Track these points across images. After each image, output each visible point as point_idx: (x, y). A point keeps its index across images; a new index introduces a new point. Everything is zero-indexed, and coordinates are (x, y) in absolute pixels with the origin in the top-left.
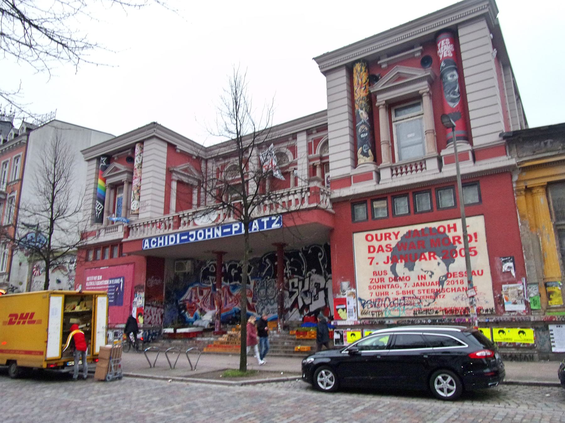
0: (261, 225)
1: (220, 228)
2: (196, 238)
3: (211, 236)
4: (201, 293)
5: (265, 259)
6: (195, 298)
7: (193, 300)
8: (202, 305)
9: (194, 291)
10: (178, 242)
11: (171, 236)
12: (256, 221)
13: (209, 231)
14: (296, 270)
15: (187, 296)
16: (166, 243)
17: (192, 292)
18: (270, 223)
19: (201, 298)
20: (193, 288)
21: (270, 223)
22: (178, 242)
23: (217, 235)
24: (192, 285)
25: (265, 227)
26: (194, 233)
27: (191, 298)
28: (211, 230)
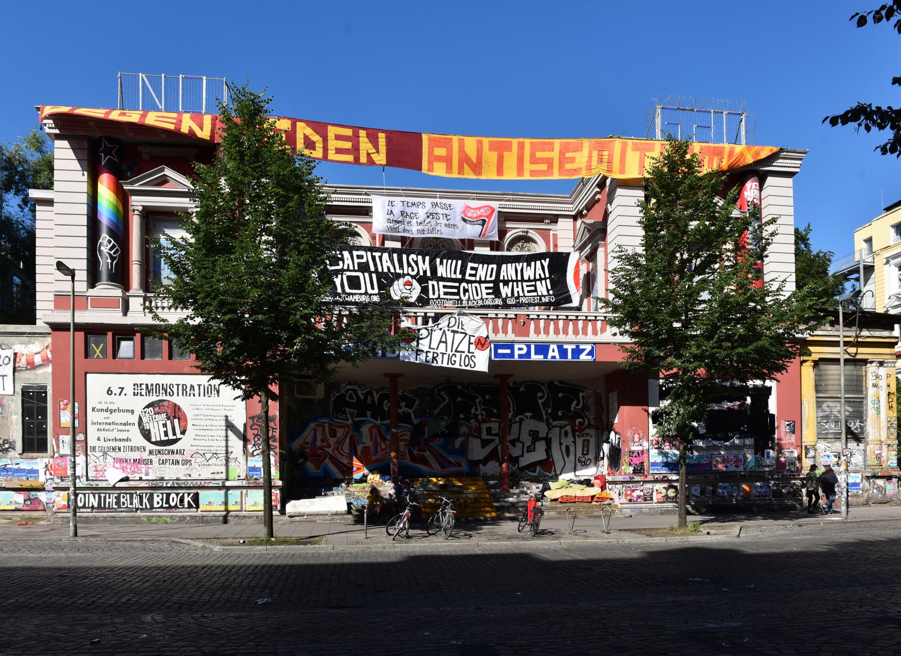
4: (333, 434)
5: (439, 391)
6: (322, 441)
7: (319, 443)
8: (336, 452)
9: (320, 429)
14: (495, 411)
15: (307, 435)
17: (315, 430)
19: (332, 441)
20: (317, 425)
24: (315, 420)
27: (315, 439)
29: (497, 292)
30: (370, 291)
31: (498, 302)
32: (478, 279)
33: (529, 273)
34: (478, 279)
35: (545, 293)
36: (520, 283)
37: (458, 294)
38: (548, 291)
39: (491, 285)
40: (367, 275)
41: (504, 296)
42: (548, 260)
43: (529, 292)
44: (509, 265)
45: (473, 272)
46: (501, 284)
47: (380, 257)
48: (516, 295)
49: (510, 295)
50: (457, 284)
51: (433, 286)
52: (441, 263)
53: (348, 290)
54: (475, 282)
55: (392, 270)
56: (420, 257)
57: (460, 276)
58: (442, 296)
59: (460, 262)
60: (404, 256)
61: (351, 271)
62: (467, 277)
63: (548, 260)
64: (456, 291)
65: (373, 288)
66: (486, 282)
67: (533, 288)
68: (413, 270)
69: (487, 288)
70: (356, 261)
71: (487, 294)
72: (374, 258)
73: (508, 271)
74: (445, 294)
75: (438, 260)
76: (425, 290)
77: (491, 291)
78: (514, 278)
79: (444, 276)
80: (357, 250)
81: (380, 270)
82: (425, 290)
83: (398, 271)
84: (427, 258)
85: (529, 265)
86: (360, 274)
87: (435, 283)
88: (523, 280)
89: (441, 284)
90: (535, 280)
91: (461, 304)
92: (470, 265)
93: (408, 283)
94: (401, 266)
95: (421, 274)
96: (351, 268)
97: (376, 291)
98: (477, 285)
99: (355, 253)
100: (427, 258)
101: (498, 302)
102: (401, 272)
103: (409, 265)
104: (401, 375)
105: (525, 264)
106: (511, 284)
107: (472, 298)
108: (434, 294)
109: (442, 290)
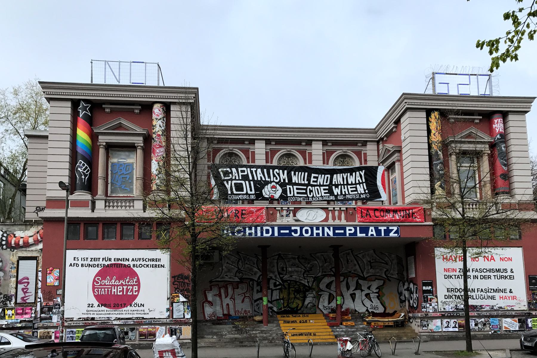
0: (378, 232)
1: (331, 228)
2: (301, 234)
3: (321, 235)
10: (276, 234)
11: (265, 228)
12: (373, 228)
13: (318, 229)
16: (259, 234)
18: (388, 231)
21: (388, 231)
22: (276, 234)
23: (328, 234)
25: (383, 235)
26: (298, 229)
28: (321, 228)
29: (331, 192)
30: (249, 192)
31: (332, 198)
32: (318, 184)
33: (351, 180)
34: (318, 184)
35: (363, 192)
36: (346, 186)
37: (306, 193)
38: (365, 190)
39: (327, 188)
40: (247, 182)
41: (336, 194)
42: (364, 171)
43: (352, 191)
44: (339, 175)
45: (316, 180)
46: (334, 187)
47: (256, 171)
48: (344, 193)
49: (339, 194)
50: (305, 187)
51: (290, 188)
52: (295, 174)
53: (235, 192)
54: (317, 185)
55: (264, 179)
56: (281, 171)
57: (307, 182)
58: (296, 195)
59: (306, 174)
60: (271, 171)
61: (237, 180)
62: (312, 183)
63: (364, 171)
64: (304, 191)
65: (251, 190)
66: (323, 185)
67: (355, 189)
68: (277, 179)
69: (324, 189)
70: (240, 174)
71: (325, 193)
72: (252, 172)
73: (338, 178)
74: (298, 193)
75: (293, 173)
76: (284, 191)
77: (327, 191)
78: (342, 183)
79: (297, 182)
80: (242, 167)
81: (256, 179)
82: (284, 191)
83: (267, 179)
84: (286, 172)
85: (351, 174)
86: (243, 182)
87: (291, 187)
88: (348, 184)
89: (295, 187)
90: (356, 184)
91: (308, 199)
92: (313, 175)
93: (273, 187)
94: (269, 177)
95: (282, 181)
96: (237, 178)
97: (253, 192)
98: (318, 188)
99: (240, 169)
100: (286, 172)
101: (332, 198)
102: (269, 180)
103: (274, 176)
104: (269, 246)
105: (349, 174)
106: (340, 187)
107: (315, 196)
108: (290, 193)
109: (296, 191)
